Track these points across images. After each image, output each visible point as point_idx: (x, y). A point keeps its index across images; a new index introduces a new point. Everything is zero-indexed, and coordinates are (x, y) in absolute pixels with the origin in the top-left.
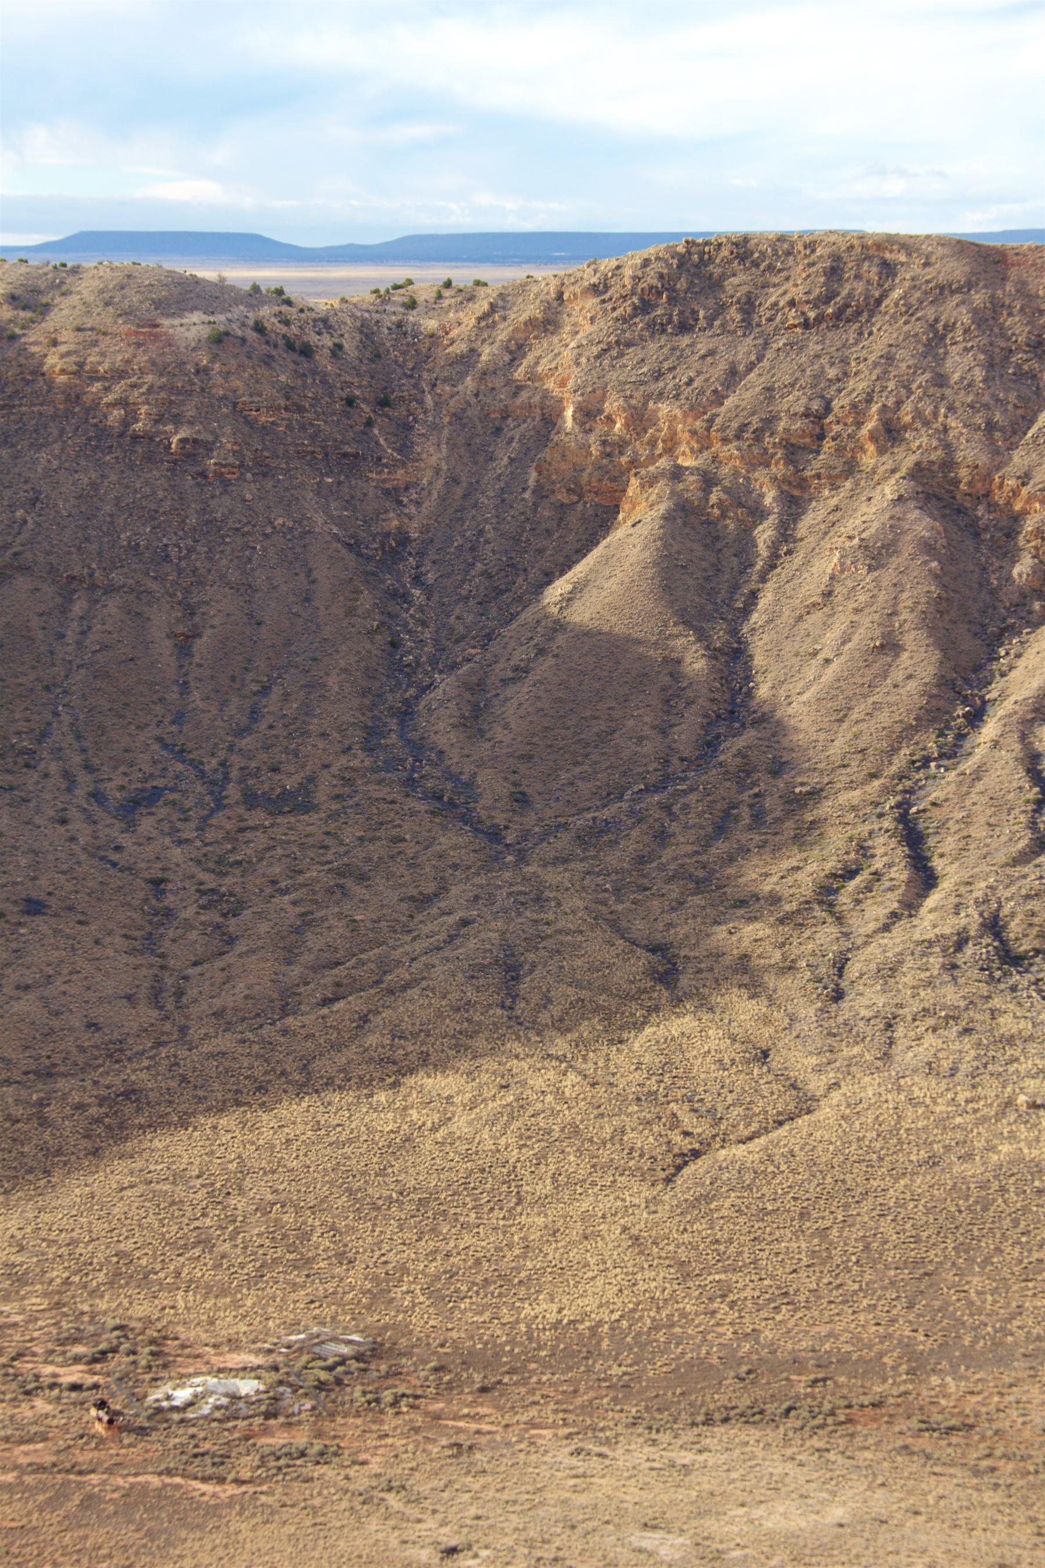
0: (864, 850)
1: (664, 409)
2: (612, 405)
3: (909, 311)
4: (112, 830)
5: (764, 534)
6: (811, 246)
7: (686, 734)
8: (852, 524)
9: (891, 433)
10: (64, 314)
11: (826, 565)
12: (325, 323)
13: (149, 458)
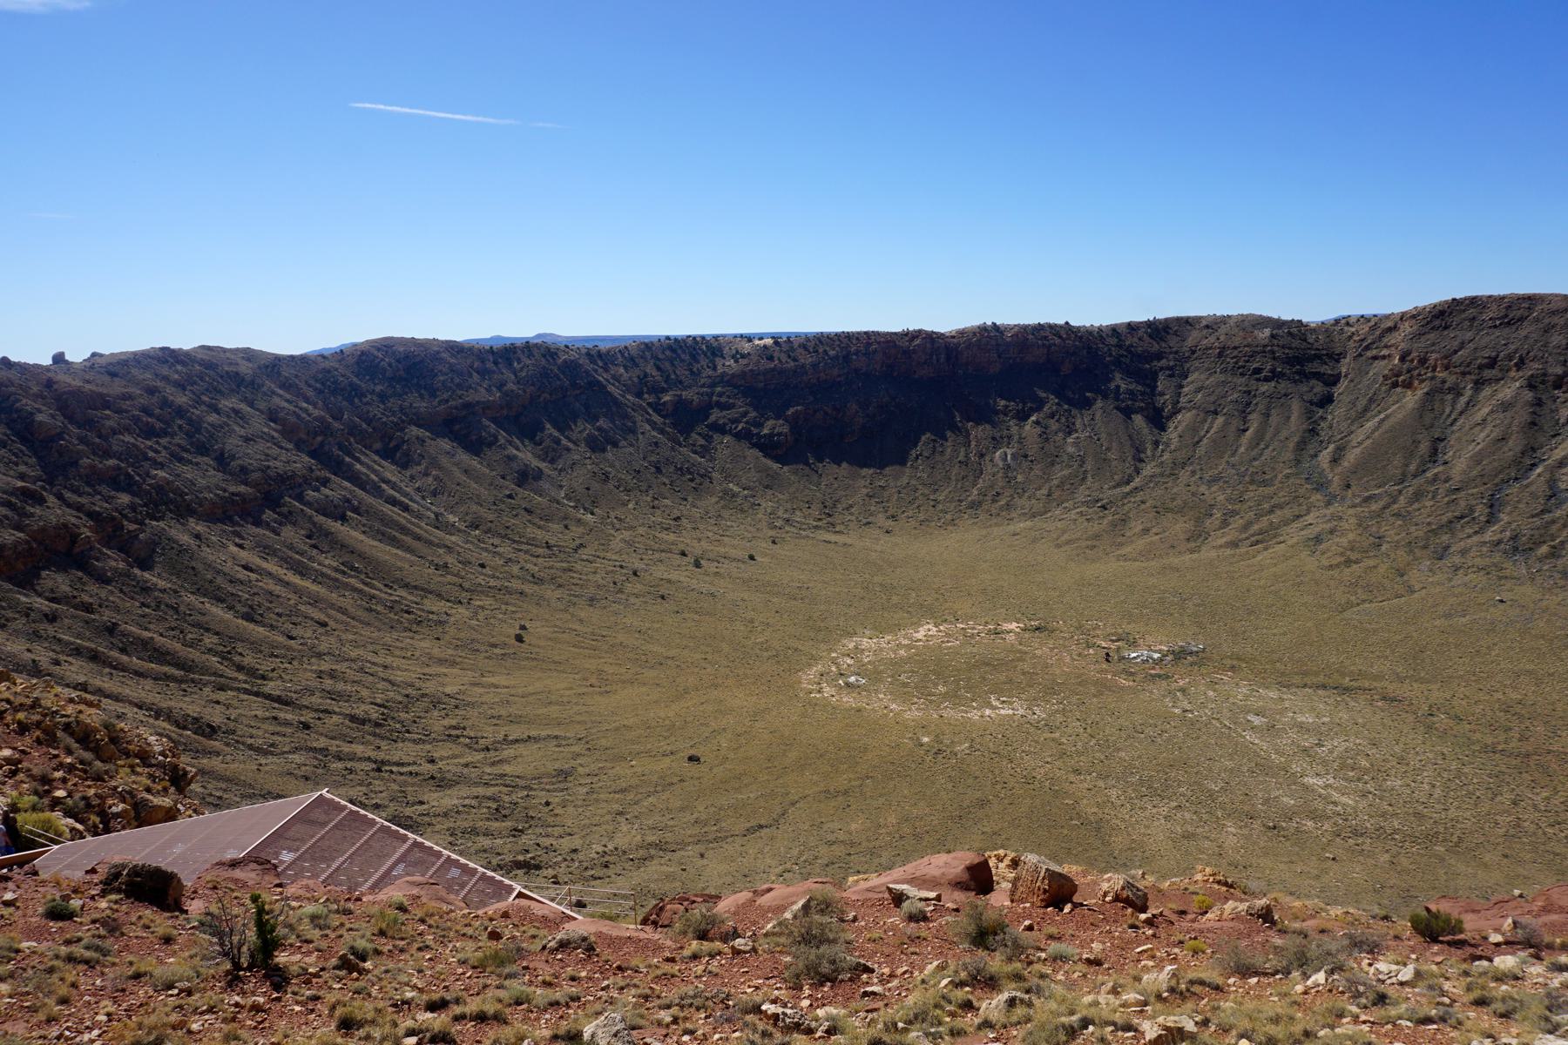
0: (1472, 510)
1: (1434, 356)
2: (1414, 354)
3: (1537, 320)
4: (1203, 489)
5: (1463, 400)
6: (1503, 298)
7: (1412, 468)
8: (1500, 396)
9: (1520, 365)
10: (1223, 329)
11: (1486, 410)
12: (1314, 330)
13: (1242, 375)
